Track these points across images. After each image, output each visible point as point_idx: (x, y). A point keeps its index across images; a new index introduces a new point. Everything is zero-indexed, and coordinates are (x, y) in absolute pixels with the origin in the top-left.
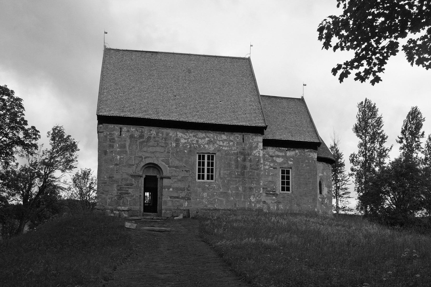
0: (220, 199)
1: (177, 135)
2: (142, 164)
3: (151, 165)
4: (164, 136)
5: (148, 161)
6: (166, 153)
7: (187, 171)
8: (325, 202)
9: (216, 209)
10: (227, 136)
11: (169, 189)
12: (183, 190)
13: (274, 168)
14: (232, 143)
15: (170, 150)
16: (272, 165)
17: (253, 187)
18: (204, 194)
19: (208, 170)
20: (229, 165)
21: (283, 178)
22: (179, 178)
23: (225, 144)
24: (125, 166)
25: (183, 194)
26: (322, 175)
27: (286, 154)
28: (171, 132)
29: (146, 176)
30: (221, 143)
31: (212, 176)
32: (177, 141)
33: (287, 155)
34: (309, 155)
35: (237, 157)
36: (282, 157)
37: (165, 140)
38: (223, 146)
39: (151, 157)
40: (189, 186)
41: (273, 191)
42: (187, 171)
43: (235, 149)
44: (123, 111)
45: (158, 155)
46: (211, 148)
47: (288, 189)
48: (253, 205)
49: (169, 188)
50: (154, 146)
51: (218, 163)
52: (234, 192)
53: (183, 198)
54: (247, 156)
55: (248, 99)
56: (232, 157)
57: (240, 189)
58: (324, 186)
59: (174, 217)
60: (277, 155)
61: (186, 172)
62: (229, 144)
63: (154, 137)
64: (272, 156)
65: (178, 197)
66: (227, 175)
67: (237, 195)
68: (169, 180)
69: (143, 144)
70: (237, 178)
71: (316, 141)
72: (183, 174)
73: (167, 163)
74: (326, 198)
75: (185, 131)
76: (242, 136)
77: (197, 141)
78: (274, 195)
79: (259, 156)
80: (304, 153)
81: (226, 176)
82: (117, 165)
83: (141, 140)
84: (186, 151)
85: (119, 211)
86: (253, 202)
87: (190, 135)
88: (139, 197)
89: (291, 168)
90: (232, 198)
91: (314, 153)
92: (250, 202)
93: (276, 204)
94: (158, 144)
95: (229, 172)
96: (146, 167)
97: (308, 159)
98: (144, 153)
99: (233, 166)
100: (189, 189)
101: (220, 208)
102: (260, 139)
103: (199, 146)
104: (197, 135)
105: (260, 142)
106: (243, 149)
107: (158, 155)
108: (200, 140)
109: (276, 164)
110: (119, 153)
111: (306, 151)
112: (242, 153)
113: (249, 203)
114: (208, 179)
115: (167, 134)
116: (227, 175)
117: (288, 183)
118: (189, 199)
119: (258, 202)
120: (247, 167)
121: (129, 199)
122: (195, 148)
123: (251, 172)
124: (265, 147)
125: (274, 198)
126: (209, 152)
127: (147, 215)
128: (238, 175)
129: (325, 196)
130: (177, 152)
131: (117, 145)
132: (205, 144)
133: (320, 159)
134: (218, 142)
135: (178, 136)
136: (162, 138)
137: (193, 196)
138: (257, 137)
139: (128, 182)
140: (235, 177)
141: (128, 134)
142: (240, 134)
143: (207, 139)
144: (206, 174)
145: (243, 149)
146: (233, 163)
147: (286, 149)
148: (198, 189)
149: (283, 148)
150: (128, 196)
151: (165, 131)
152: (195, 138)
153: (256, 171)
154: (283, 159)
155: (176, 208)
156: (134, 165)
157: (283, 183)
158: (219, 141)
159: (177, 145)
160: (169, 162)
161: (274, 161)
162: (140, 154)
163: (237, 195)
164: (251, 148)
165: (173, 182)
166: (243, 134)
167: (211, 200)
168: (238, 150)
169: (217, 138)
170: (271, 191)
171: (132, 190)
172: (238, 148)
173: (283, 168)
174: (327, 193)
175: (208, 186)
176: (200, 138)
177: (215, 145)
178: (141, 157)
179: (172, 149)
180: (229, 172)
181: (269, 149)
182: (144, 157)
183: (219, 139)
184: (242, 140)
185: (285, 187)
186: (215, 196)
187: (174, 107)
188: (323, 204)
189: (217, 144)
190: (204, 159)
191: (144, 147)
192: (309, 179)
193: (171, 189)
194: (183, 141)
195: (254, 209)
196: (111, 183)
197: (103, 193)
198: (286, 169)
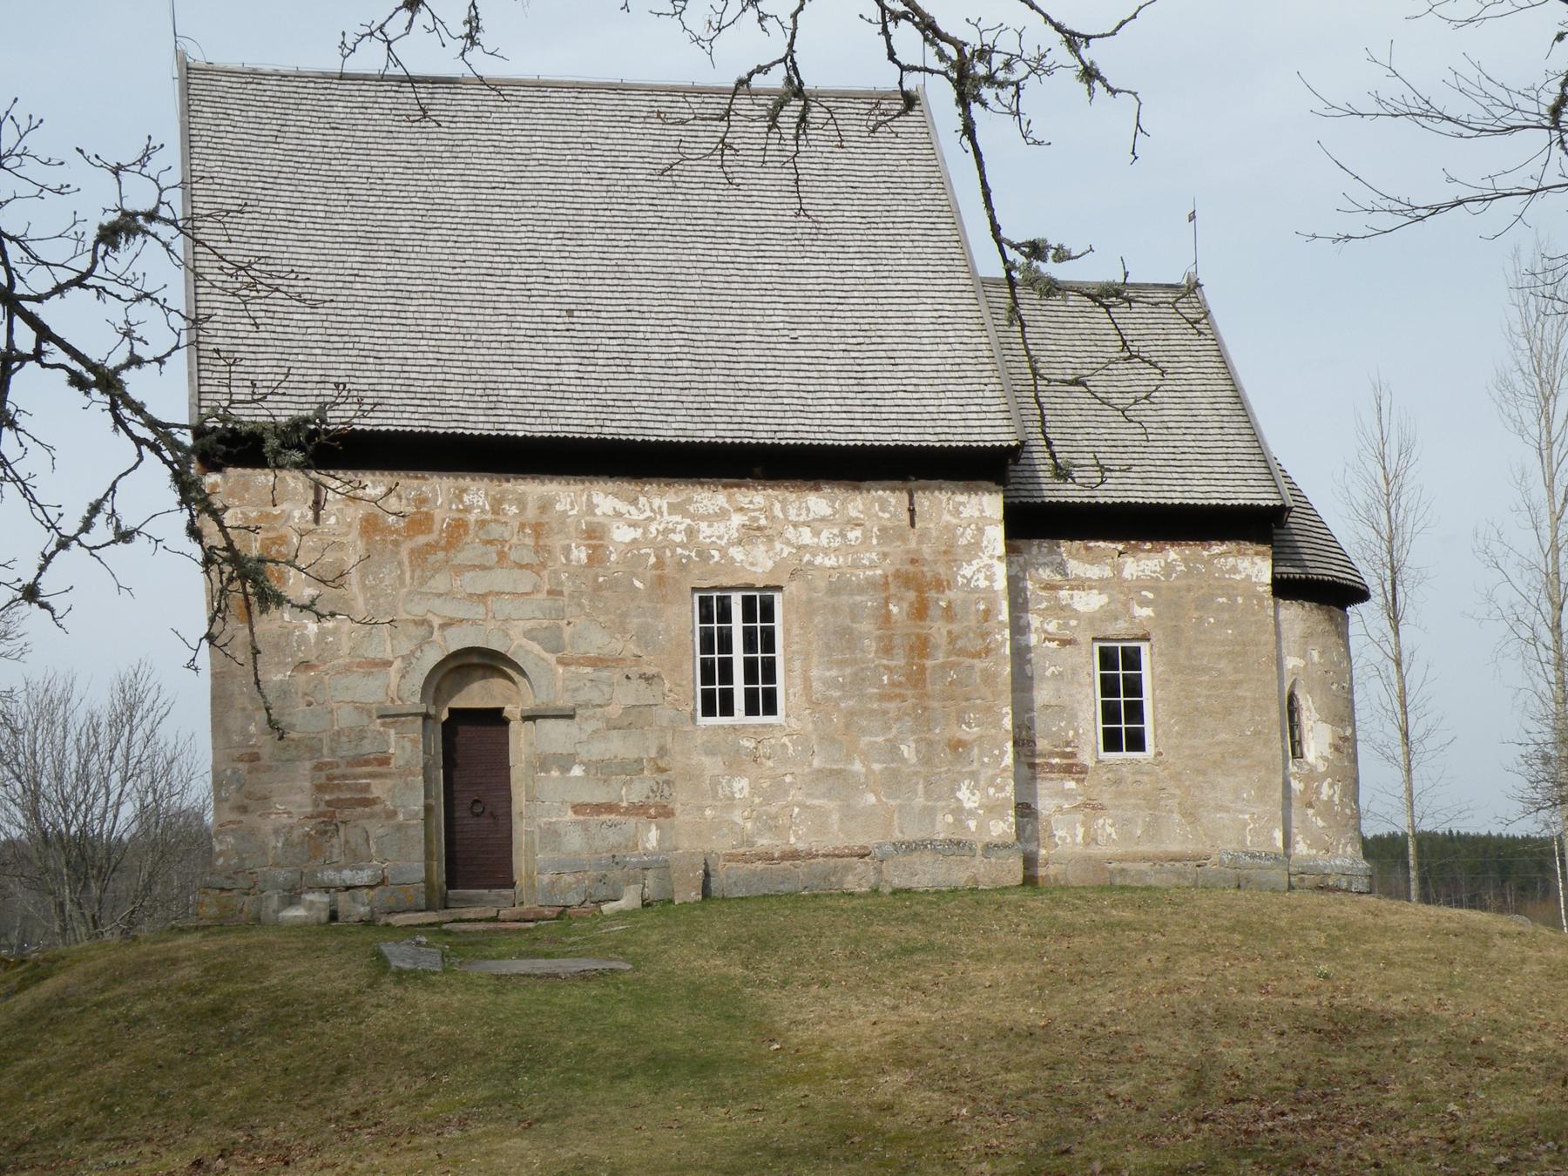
0: (816, 802)
1: (591, 507)
2: (432, 657)
3: (475, 660)
4: (531, 513)
5: (458, 640)
6: (543, 595)
8: (1324, 797)
9: (794, 855)
11: (566, 769)
12: (632, 768)
13: (1065, 643)
14: (858, 533)
15: (561, 583)
16: (1052, 627)
17: (966, 737)
18: (737, 785)
20: (847, 638)
21: (1109, 686)
22: (615, 711)
23: (824, 541)
24: (347, 669)
25: (634, 793)
26: (1301, 663)
27: (1118, 569)
28: (566, 497)
29: (451, 711)
30: (806, 536)
31: (770, 696)
32: (594, 535)
33: (1126, 574)
34: (1234, 570)
35: (887, 601)
36: (1102, 585)
37: (538, 535)
38: (815, 550)
39: (474, 622)
40: (662, 751)
41: (1064, 755)
43: (874, 563)
45: (505, 607)
46: (757, 564)
47: (1137, 742)
48: (972, 824)
50: (484, 568)
51: (795, 631)
52: (877, 767)
53: (638, 809)
54: (933, 594)
55: (924, 314)
56: (858, 598)
57: (908, 751)
59: (598, 903)
60: (1077, 578)
61: (643, 683)
62: (843, 535)
63: (482, 524)
65: (610, 808)
66: (842, 686)
67: (894, 780)
68: (562, 723)
69: (431, 559)
70: (890, 698)
71: (1266, 498)
72: (627, 695)
73: (554, 643)
74: (1324, 776)
75: (628, 487)
76: (905, 496)
77: (690, 532)
78: (1068, 770)
79: (990, 589)
80: (1209, 562)
81: (836, 694)
82: (305, 665)
83: (421, 540)
84: (637, 584)
85: (327, 889)
87: (656, 502)
88: (422, 815)
89: (1146, 638)
90: (871, 799)
91: (1257, 559)
92: (958, 811)
93: (1080, 817)
94: (502, 556)
95: (848, 671)
96: (451, 671)
97: (1230, 590)
98: (438, 602)
99: (870, 645)
100: (662, 764)
102: (988, 506)
103: (704, 555)
104: (690, 500)
105: (991, 521)
106: (913, 561)
108: (703, 525)
109: (1073, 623)
111: (1217, 548)
112: (906, 580)
113: (950, 819)
114: (751, 709)
115: (545, 506)
116: (842, 686)
117: (1135, 712)
118: (666, 812)
119: (992, 809)
120: (937, 647)
121: (377, 829)
122: (682, 567)
123: (953, 666)
124: (1020, 543)
125: (1071, 785)
126: (749, 580)
127: (469, 902)
128: (892, 684)
129: (1322, 768)
130: (598, 588)
132: (731, 544)
133: (1284, 588)
134: (790, 533)
135: (598, 512)
136: (522, 526)
137: (680, 799)
138: (974, 499)
139: (368, 747)
140: (883, 697)
141: (356, 513)
142: (893, 490)
143: (737, 520)
144: (739, 686)
145: (913, 561)
146: (866, 626)
147: (1120, 547)
148: (707, 761)
149: (1102, 544)
150: (371, 816)
151: (533, 489)
152: (678, 518)
153: (979, 664)
154: (1104, 599)
156: (389, 664)
157: (1110, 713)
158: (795, 526)
159: (597, 556)
160: (560, 637)
161: (1063, 608)
162: (418, 610)
163: (894, 780)
164: (951, 554)
165: (584, 737)
166: (912, 484)
167: (773, 810)
168: (888, 566)
169: (784, 510)
170: (1052, 754)
171: (389, 782)
172: (885, 555)
174: (1328, 752)
175: (750, 744)
176: (703, 518)
177: (778, 546)
178: (423, 622)
179: (573, 576)
180: (848, 671)
181: (1035, 550)
182: (436, 622)
183: (792, 518)
184: (906, 516)
185: (1123, 728)
186: (786, 793)
187: (569, 371)
188: (1310, 805)
189: (788, 543)
190: (725, 616)
191: (437, 571)
192: (1236, 684)
193: (577, 771)
194: (622, 534)
196: (285, 756)
197: (243, 809)
198: (1120, 645)
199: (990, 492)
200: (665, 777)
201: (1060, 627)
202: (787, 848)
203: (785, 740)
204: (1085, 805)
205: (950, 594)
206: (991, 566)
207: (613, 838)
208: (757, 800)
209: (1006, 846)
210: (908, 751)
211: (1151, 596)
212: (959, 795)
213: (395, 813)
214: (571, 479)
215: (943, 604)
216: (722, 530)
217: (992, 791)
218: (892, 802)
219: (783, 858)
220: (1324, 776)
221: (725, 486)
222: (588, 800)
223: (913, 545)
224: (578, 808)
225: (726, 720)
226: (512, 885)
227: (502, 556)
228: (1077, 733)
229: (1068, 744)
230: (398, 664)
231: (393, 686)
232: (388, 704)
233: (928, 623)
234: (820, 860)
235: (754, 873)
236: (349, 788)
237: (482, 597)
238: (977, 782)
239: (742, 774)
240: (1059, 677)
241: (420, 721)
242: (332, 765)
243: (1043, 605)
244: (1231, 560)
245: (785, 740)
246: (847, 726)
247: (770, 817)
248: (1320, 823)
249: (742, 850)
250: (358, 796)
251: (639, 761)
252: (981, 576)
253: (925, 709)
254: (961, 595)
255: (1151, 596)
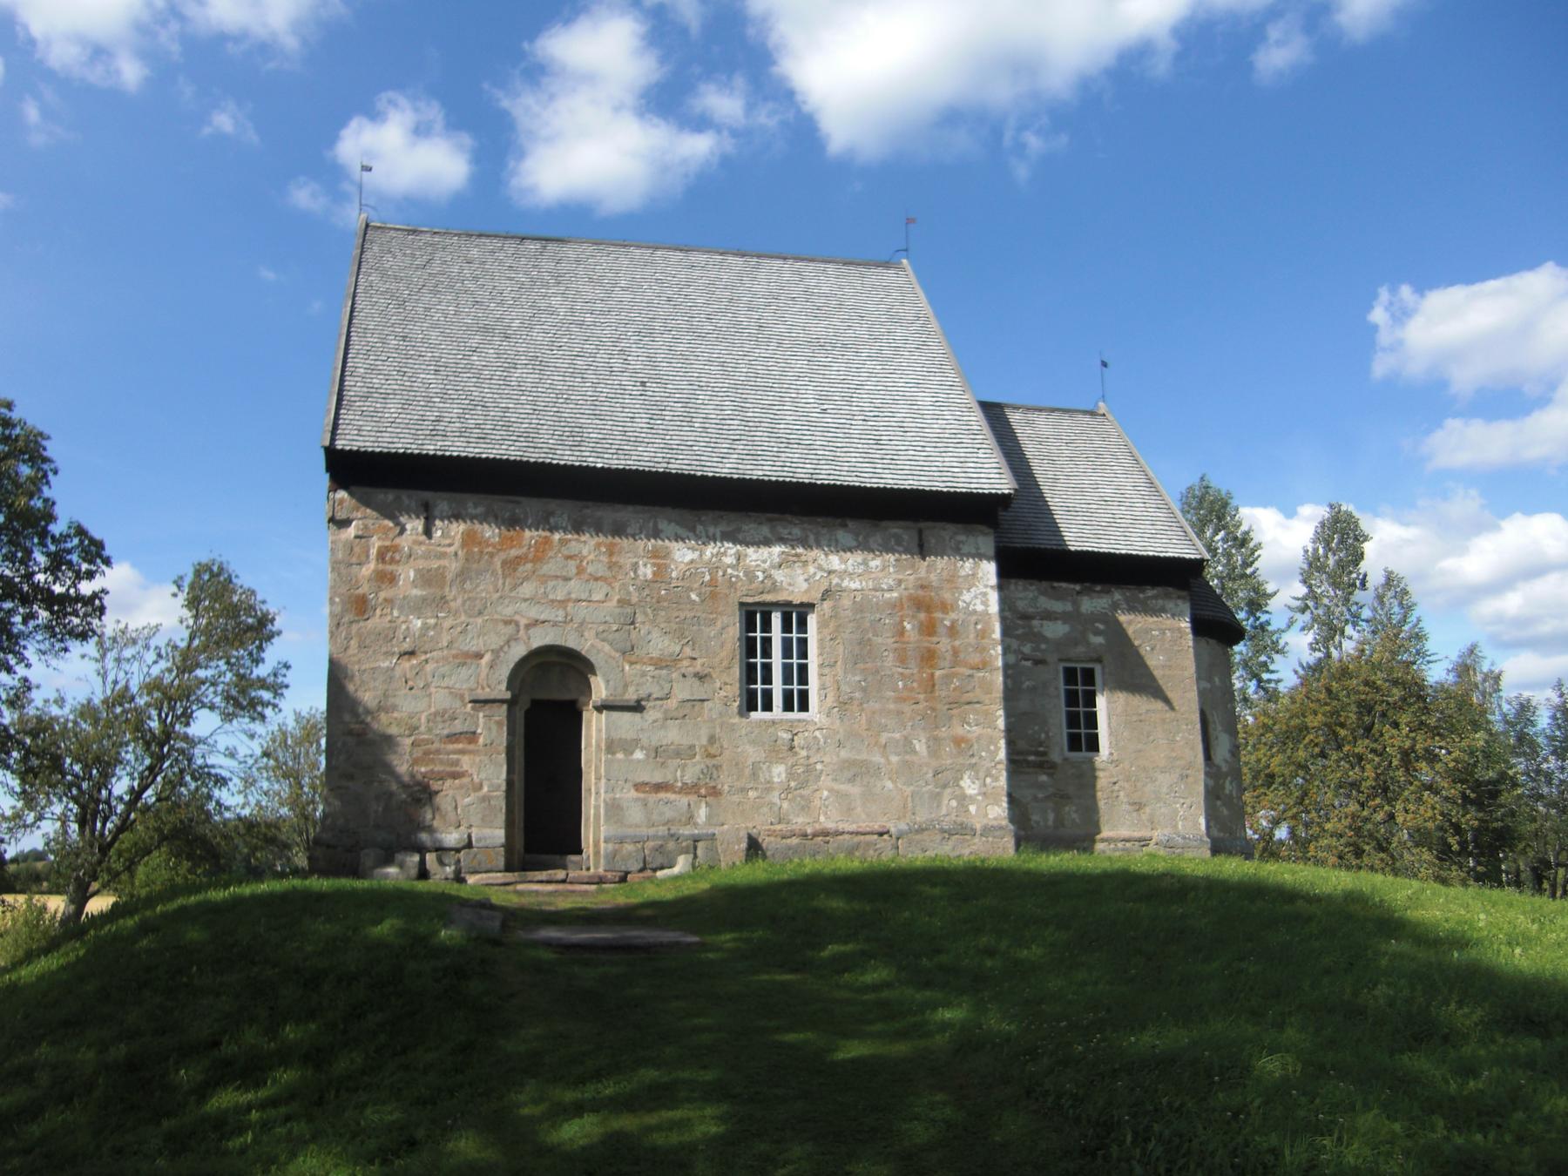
2: (519, 651)
3: (554, 658)
5: (540, 639)
6: (614, 603)
7: (701, 677)
9: (825, 833)
10: (857, 535)
13: (1037, 662)
15: (629, 593)
16: (1027, 649)
19: (787, 670)
25: (690, 774)
27: (1076, 604)
31: (804, 696)
36: (1064, 617)
37: (611, 554)
38: (844, 574)
39: (555, 624)
40: (712, 739)
42: (701, 677)
44: (434, 433)
45: (582, 611)
48: (972, 809)
49: (628, 746)
52: (894, 759)
53: (687, 789)
54: (938, 615)
55: (925, 399)
57: (920, 746)
58: (1219, 728)
59: (655, 870)
61: (695, 680)
64: (1026, 617)
69: (521, 569)
74: (1227, 775)
79: (986, 613)
86: (972, 799)
88: (504, 787)
89: (1099, 660)
90: (889, 785)
91: (1180, 602)
92: (963, 799)
94: (580, 570)
98: (524, 605)
100: (712, 751)
101: (841, 826)
103: (750, 575)
104: (739, 530)
106: (922, 587)
107: (582, 611)
109: (1043, 646)
110: (418, 607)
111: (1150, 592)
113: (954, 803)
114: (788, 707)
116: (864, 690)
118: (715, 792)
123: (955, 675)
125: (1044, 778)
129: (1225, 769)
131: (412, 574)
137: (725, 782)
138: (971, 539)
139: (458, 726)
145: (922, 587)
146: (885, 640)
147: (1078, 587)
148: (750, 749)
149: (1064, 585)
155: (662, 830)
156: (479, 656)
162: (508, 611)
163: (908, 769)
166: (922, 525)
173: (1069, 660)
174: (1228, 756)
177: (811, 569)
178: (507, 623)
179: (641, 589)
181: (1012, 587)
182: (523, 622)
187: (641, 422)
188: (1218, 798)
189: (820, 568)
190: (767, 627)
191: (526, 579)
193: (639, 755)
195: (978, 826)
197: (351, 777)
199: (986, 534)
200: (714, 762)
201: (1034, 650)
202: (817, 826)
203: (817, 733)
204: (1055, 795)
205: (953, 616)
206: (985, 594)
207: (669, 813)
208: (793, 784)
209: (1001, 828)
210: (920, 746)
211: (1101, 627)
212: (962, 783)
213: (481, 786)
214: (639, 508)
215: (947, 623)
216: (766, 555)
217: (988, 780)
218: (909, 790)
219: (815, 835)
220: (1227, 775)
221: (770, 520)
222: (647, 779)
223: (923, 573)
224: (638, 787)
225: (767, 715)
226: (580, 852)
227: (580, 570)
228: (1048, 736)
229: (1041, 744)
230: (487, 657)
231: (483, 675)
232: (479, 691)
233: (935, 639)
234: (846, 837)
235: (790, 848)
236: (442, 762)
237: (563, 603)
238: (977, 772)
239: (782, 760)
240: (1033, 689)
241: (505, 707)
242: (428, 742)
243: (1020, 632)
244: (1160, 602)
245: (817, 733)
246: (869, 722)
247: (802, 797)
248: (1225, 812)
249: (778, 827)
250: (448, 769)
251: (692, 747)
252: (978, 601)
253: (933, 709)
254: (962, 616)
255: (1101, 627)
